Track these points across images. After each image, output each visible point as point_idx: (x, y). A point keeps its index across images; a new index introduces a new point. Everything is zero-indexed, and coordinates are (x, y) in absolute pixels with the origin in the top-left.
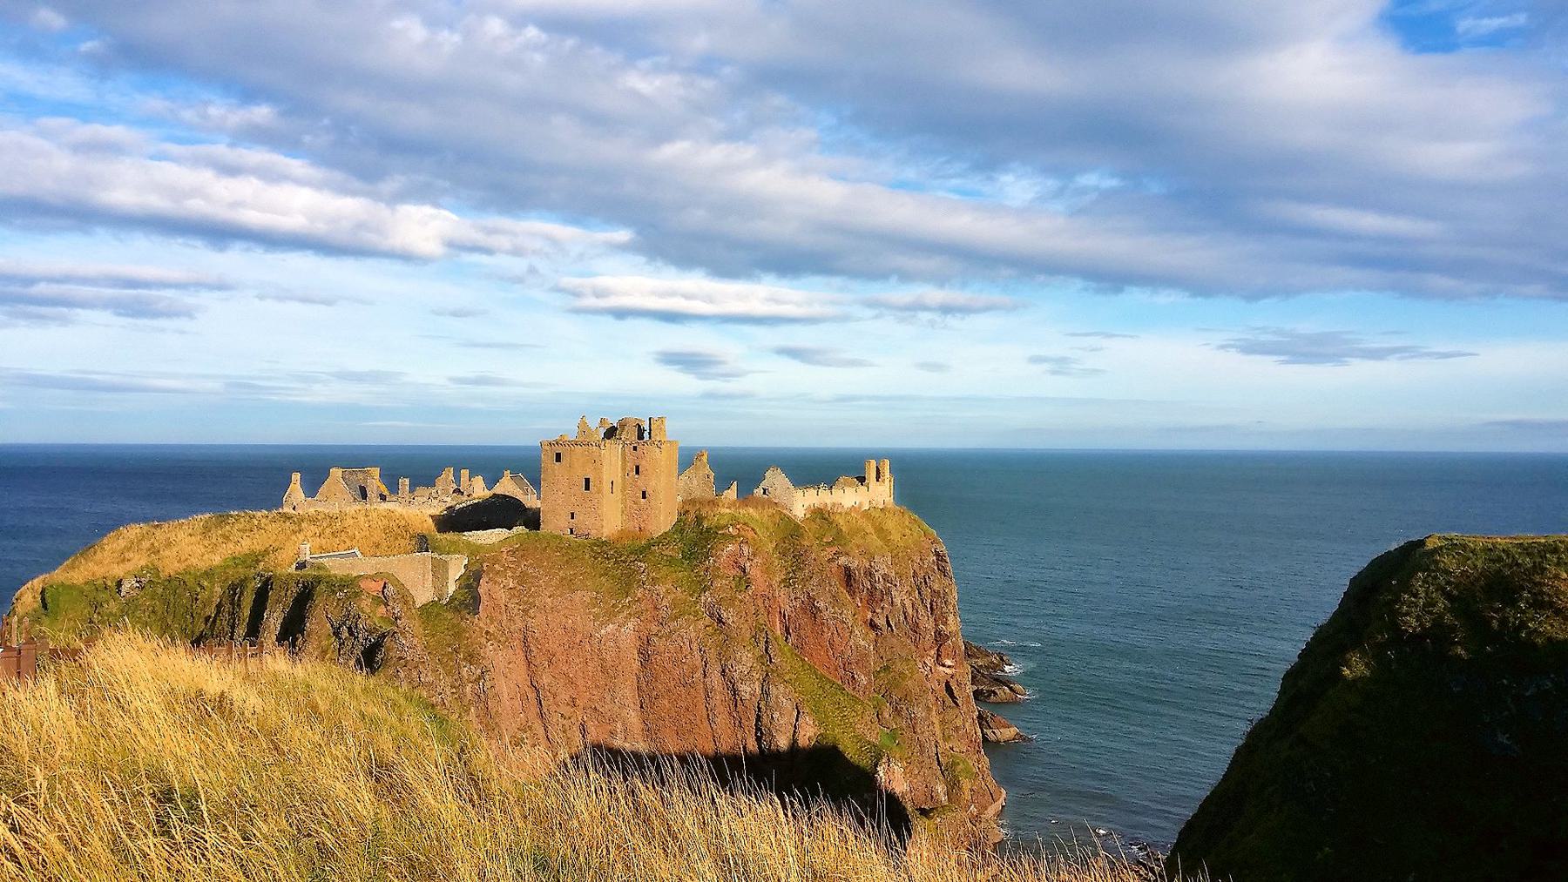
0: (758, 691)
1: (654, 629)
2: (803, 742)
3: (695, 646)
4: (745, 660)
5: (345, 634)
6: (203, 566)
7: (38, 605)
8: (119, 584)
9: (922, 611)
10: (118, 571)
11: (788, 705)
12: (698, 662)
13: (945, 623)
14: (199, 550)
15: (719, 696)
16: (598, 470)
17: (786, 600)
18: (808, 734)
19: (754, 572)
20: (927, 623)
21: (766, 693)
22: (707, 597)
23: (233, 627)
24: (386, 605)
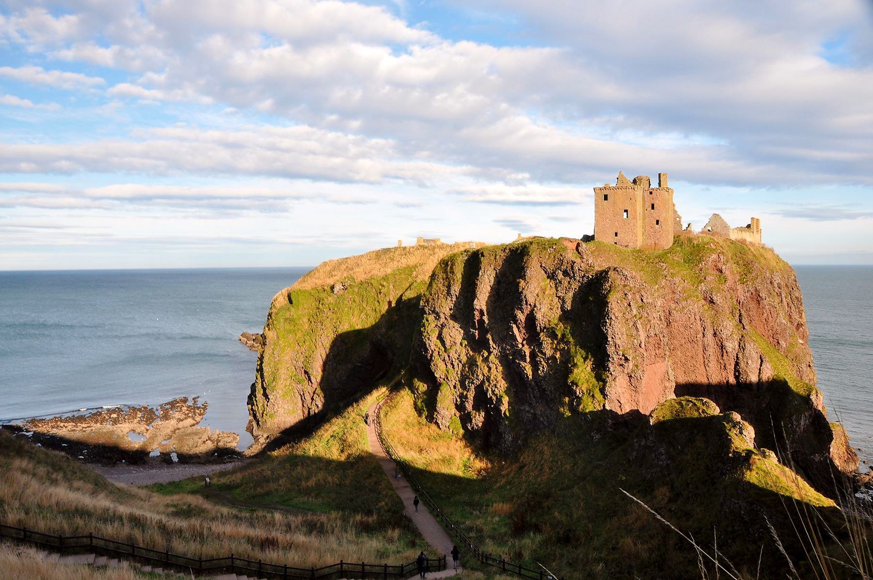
0: (737, 347)
1: (673, 306)
2: (765, 377)
3: (698, 318)
4: (729, 327)
5: (560, 276)
6: (381, 274)
7: (287, 301)
8: (332, 288)
9: (793, 308)
10: (331, 281)
11: (756, 357)
12: (700, 329)
13: (801, 317)
14: (378, 266)
15: (712, 350)
16: (634, 205)
17: (742, 293)
18: (768, 374)
19: (727, 272)
20: (796, 316)
21: (741, 347)
22: (703, 287)
23: (449, 287)
24: (582, 258)
